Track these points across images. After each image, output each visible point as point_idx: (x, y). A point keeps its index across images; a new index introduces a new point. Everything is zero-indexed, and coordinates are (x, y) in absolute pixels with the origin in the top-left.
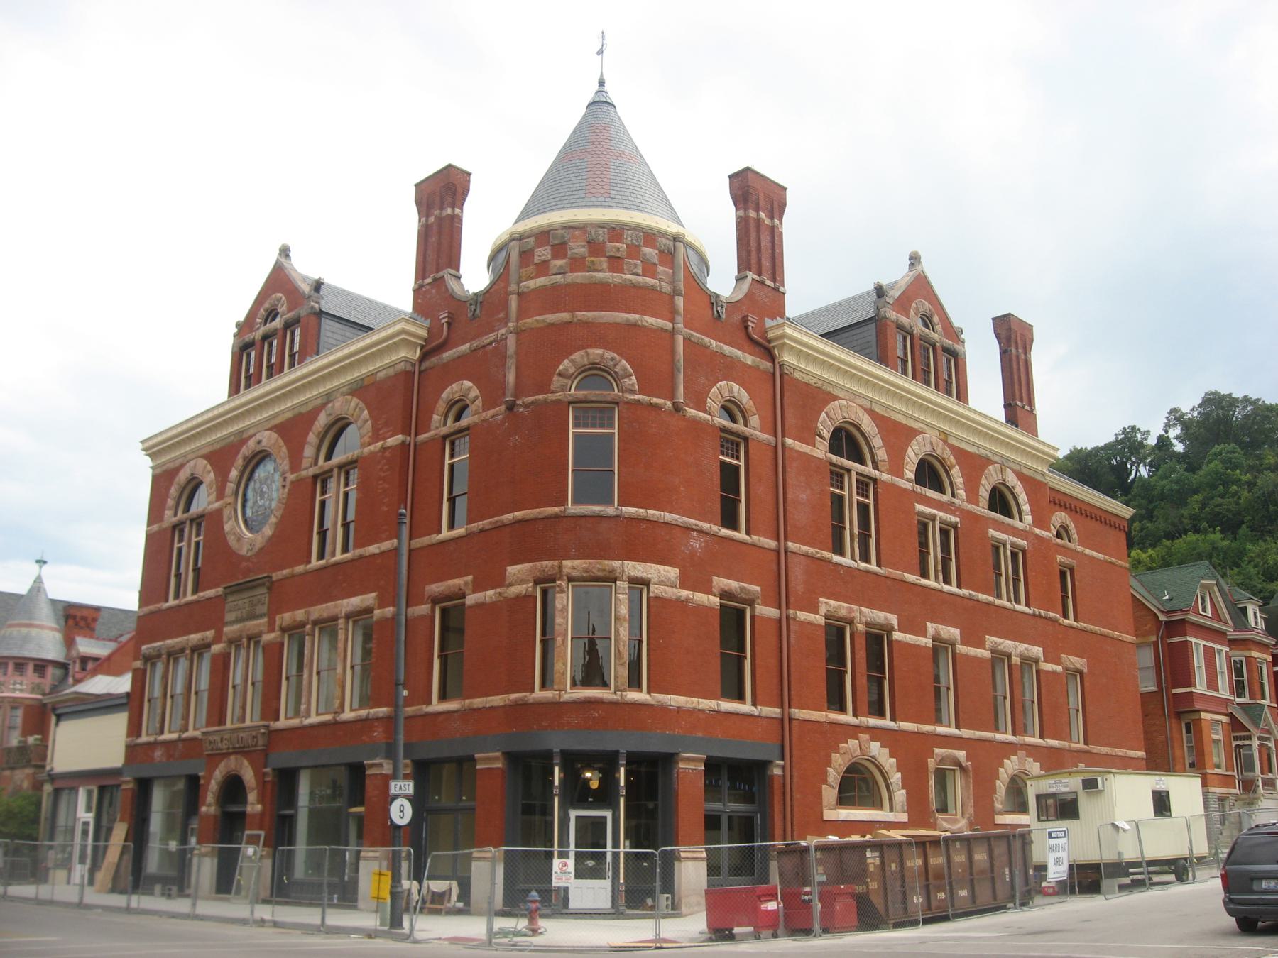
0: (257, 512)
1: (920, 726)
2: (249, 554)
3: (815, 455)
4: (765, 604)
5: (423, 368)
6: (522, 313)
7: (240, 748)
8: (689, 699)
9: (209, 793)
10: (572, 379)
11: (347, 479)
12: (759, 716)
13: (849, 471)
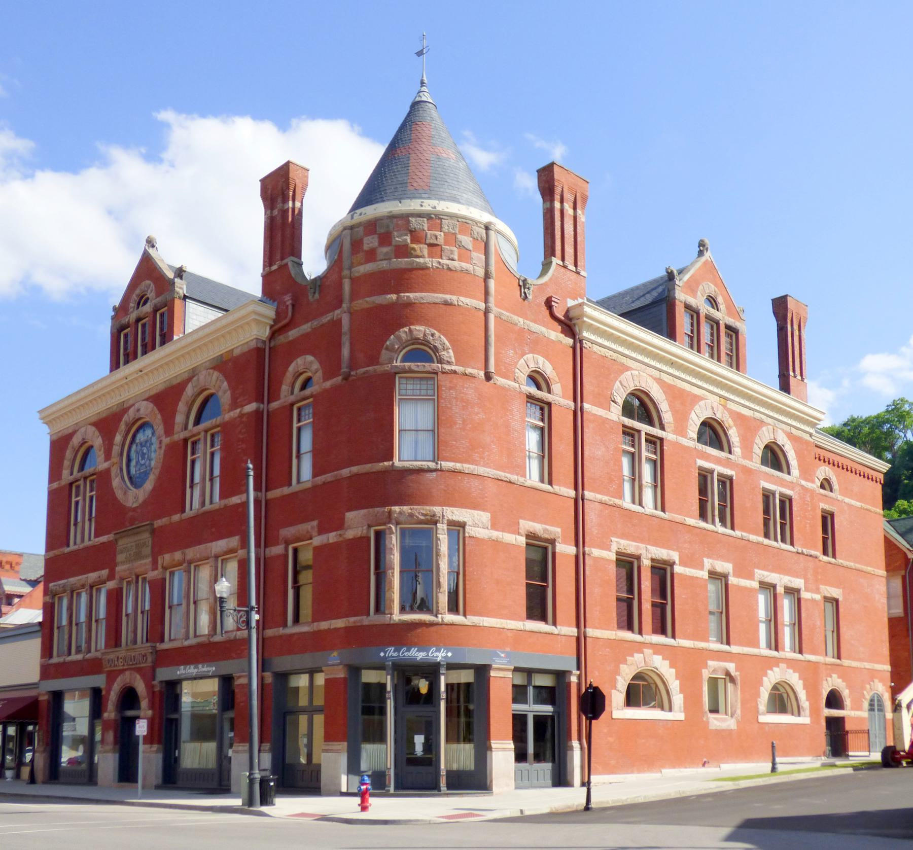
0: (139, 470)
1: (696, 643)
2: (135, 505)
3: (609, 418)
4: (565, 542)
5: (272, 344)
6: (354, 296)
7: (133, 664)
8: (499, 620)
9: (109, 702)
10: (398, 352)
11: (212, 441)
12: (558, 635)
13: (639, 431)
